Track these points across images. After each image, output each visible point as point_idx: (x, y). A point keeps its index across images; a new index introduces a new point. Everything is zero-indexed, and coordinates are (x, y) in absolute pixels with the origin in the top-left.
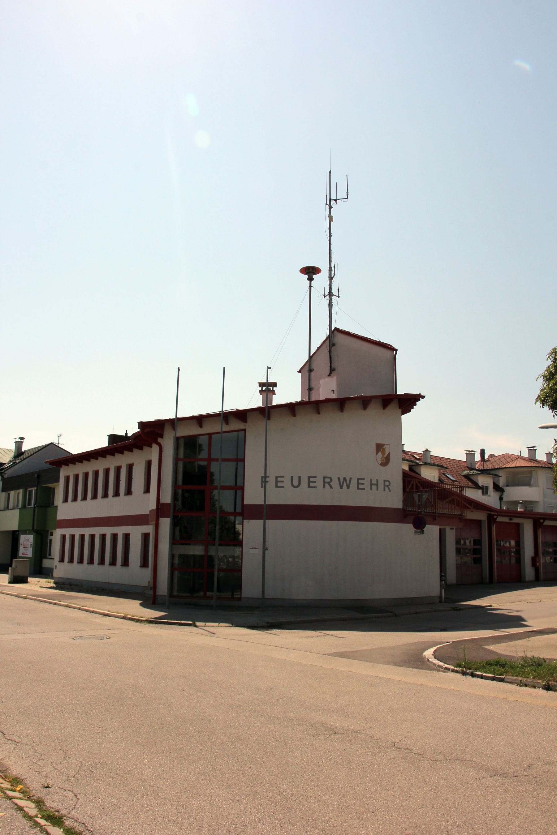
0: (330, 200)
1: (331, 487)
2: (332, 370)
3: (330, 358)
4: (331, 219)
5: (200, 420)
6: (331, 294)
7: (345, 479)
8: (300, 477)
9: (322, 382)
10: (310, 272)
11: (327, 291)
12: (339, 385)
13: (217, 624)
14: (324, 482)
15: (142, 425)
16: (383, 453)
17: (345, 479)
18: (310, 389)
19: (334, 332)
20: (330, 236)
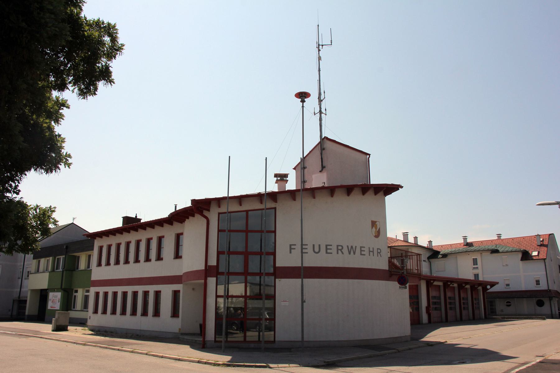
0: (319, 45)
1: (343, 253)
2: (323, 167)
3: (322, 159)
4: (320, 58)
5: (240, 199)
6: (321, 112)
7: (352, 247)
8: (319, 245)
9: (313, 176)
10: (303, 96)
11: (317, 110)
12: (328, 179)
13: (287, 365)
14: (338, 250)
15: (193, 201)
16: (376, 228)
17: (352, 247)
18: (304, 182)
19: (324, 140)
20: (319, 70)
